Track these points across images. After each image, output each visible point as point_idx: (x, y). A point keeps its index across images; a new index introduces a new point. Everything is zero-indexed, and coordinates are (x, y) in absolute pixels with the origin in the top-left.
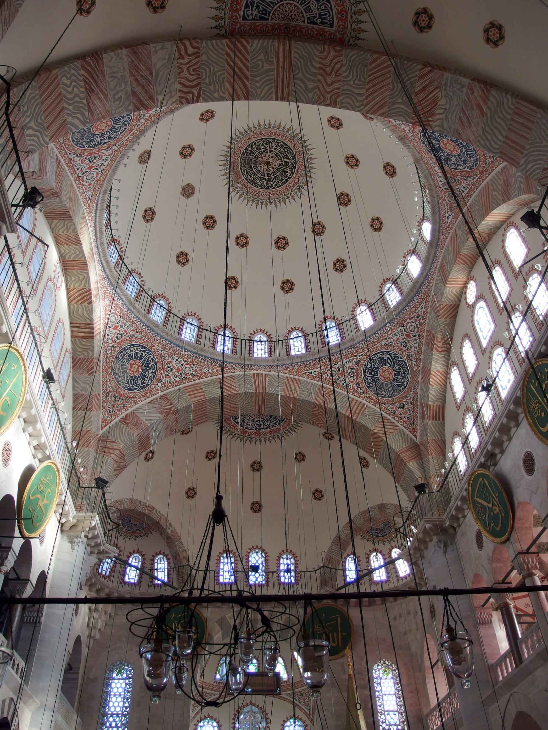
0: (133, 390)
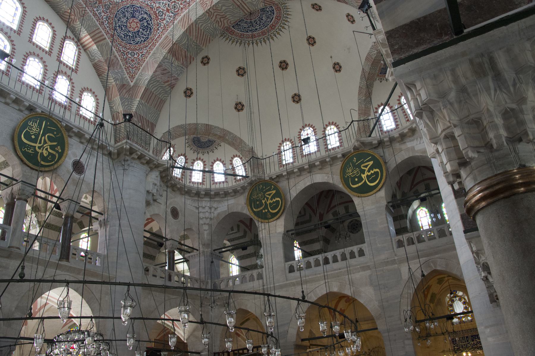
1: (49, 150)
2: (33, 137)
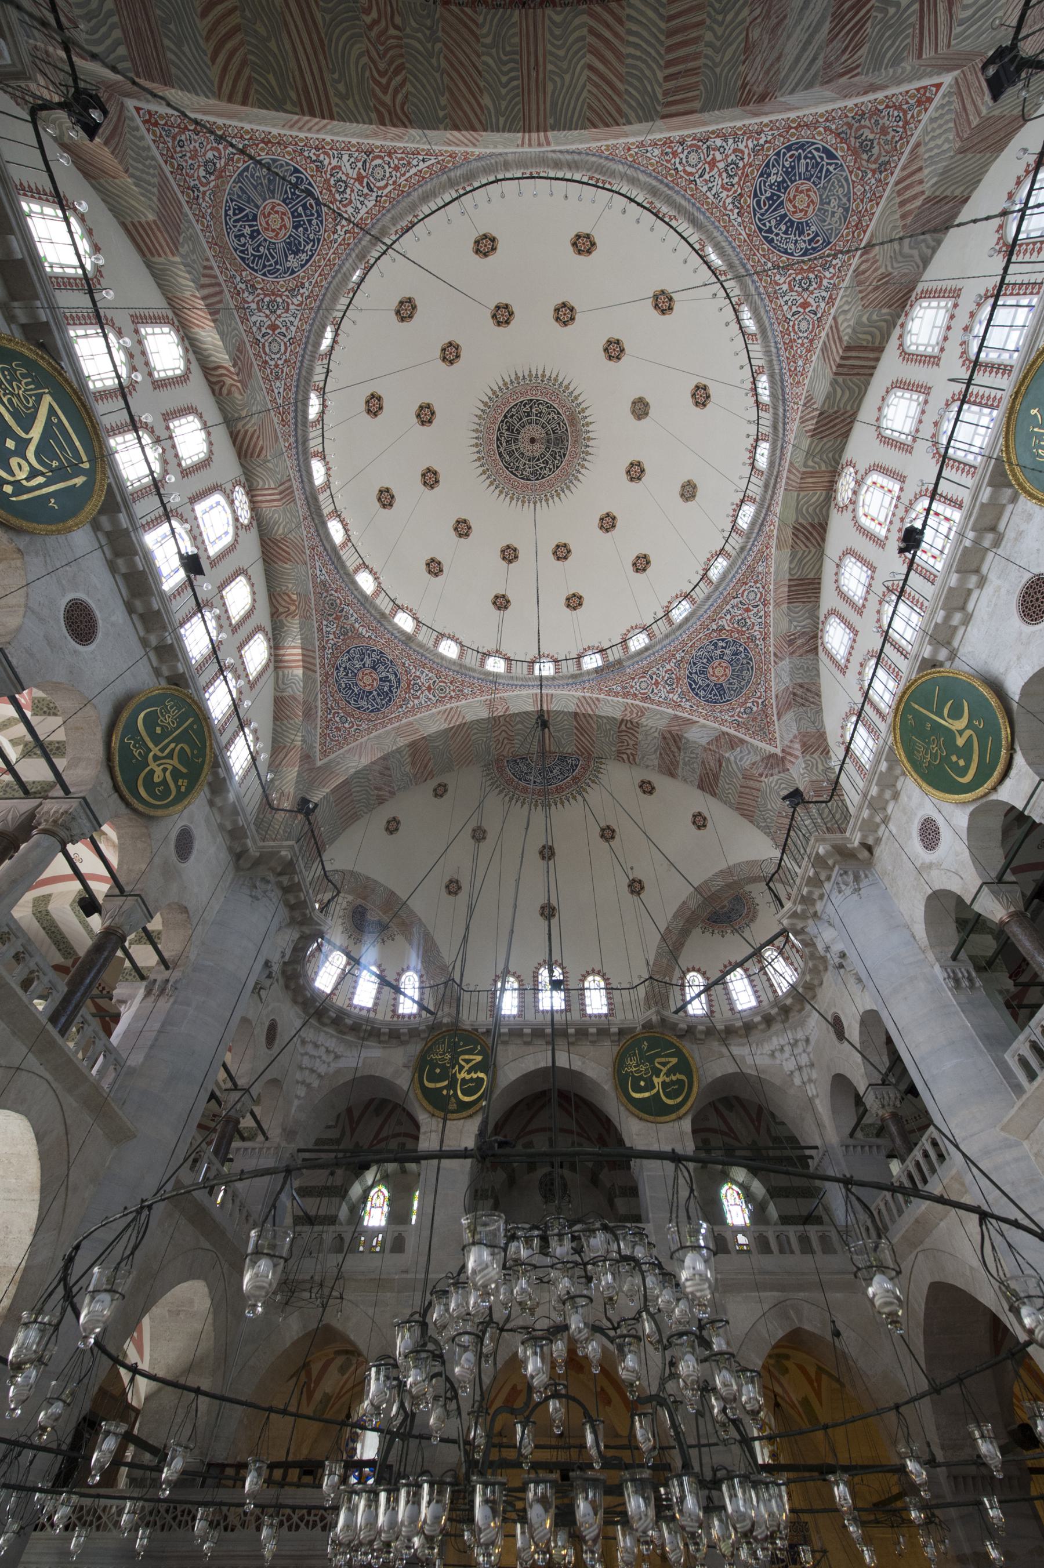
0: (826, 151)
1: (168, 773)
2: (158, 730)
